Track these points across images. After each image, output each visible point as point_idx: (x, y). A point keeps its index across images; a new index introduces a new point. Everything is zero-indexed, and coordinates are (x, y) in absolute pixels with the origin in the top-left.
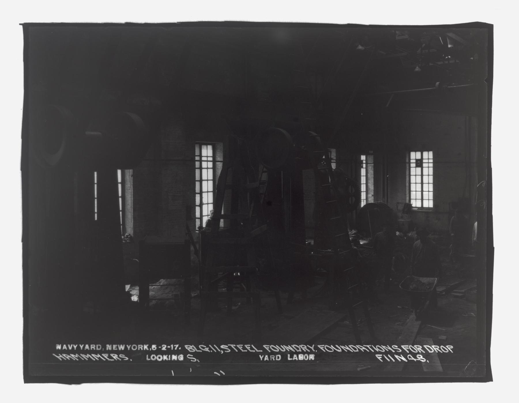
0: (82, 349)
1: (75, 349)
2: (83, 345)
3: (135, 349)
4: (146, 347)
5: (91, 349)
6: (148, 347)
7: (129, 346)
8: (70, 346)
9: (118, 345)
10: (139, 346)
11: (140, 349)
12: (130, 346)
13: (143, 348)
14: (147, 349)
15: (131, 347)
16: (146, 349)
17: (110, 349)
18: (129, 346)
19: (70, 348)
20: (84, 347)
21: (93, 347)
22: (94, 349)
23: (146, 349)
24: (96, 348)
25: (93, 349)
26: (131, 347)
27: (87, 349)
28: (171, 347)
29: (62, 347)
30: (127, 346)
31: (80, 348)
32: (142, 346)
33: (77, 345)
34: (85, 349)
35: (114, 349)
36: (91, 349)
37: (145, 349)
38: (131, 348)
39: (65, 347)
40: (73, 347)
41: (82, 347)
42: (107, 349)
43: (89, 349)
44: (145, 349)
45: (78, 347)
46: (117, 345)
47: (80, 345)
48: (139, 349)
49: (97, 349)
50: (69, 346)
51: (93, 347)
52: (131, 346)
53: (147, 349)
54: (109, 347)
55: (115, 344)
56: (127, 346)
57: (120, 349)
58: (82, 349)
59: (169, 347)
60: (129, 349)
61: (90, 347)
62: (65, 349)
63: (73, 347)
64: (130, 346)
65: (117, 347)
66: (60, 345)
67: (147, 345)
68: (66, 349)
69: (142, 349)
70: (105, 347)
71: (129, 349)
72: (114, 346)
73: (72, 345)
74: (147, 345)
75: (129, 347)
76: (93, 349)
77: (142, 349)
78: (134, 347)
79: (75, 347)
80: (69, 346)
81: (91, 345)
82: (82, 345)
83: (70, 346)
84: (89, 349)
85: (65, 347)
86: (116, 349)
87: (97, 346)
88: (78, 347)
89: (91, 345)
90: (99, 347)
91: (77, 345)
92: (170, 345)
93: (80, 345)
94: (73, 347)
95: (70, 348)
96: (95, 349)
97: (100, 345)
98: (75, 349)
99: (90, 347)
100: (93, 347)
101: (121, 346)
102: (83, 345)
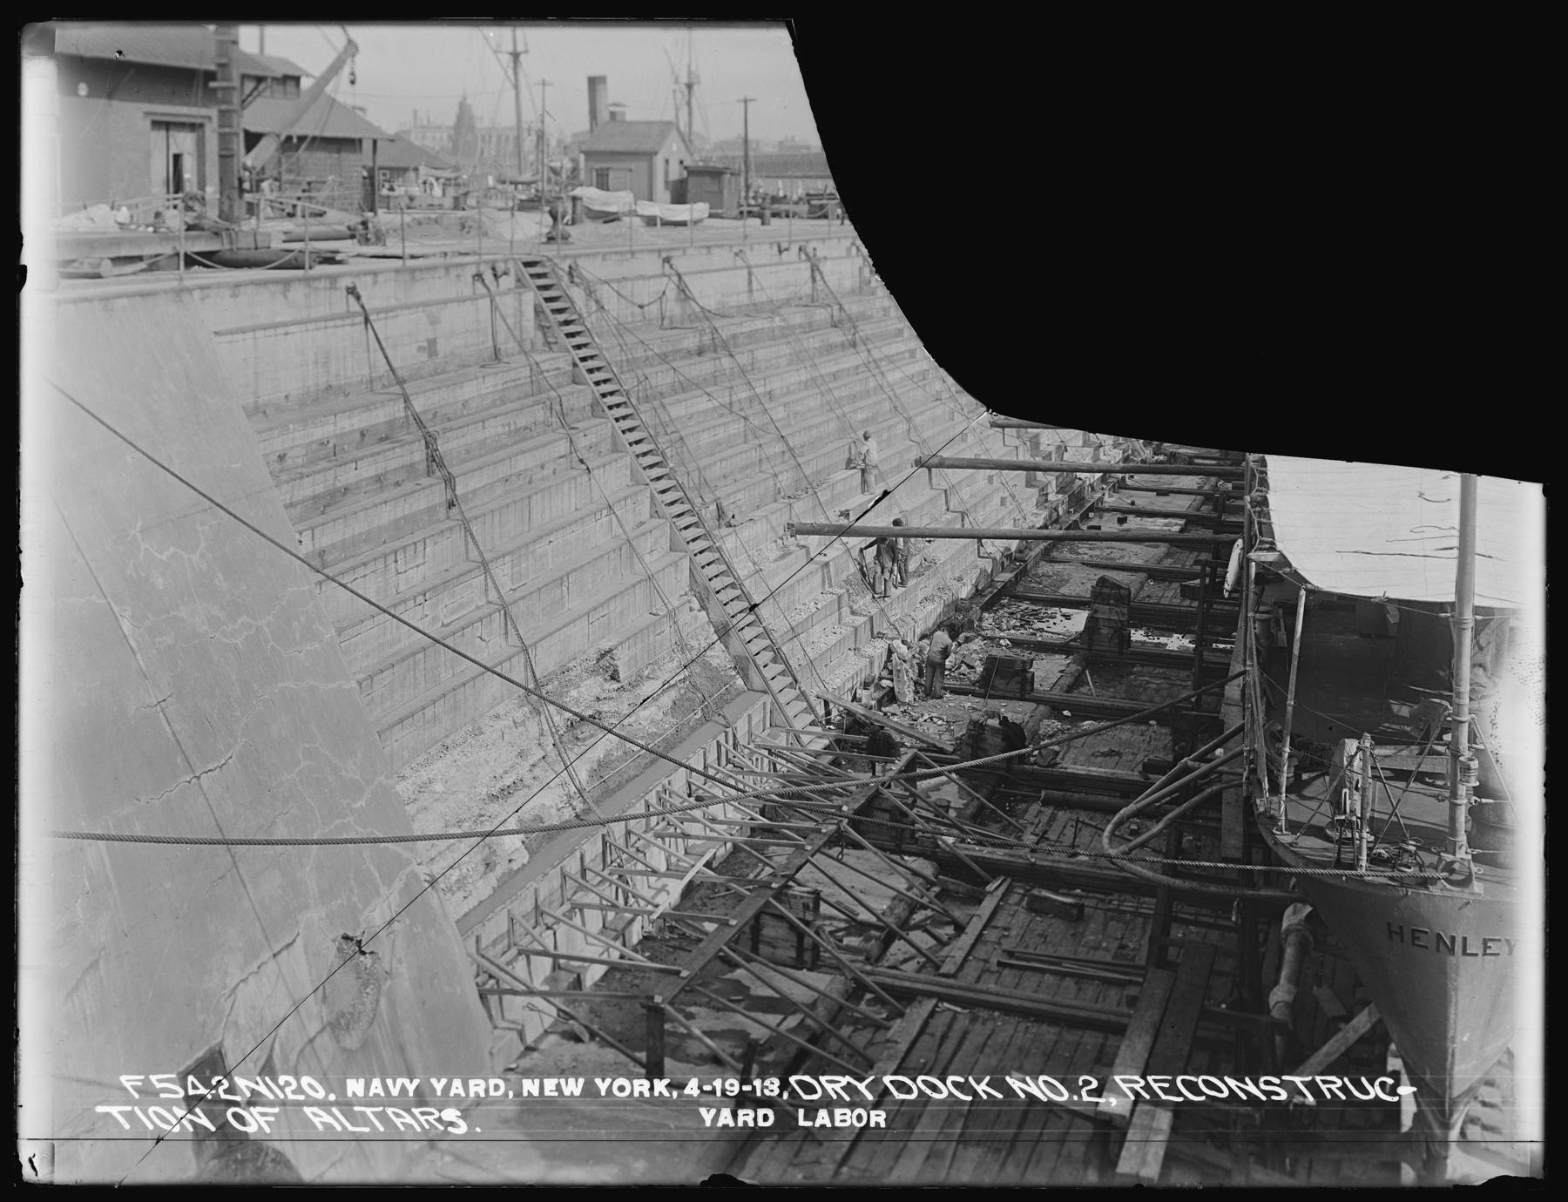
0: (439, 1093)
2: (444, 1081)
5: (472, 1095)
6: (669, 1086)
7: (603, 1080)
10: (636, 1082)
12: (608, 1081)
13: (652, 1089)
14: (666, 1094)
17: (536, 1093)
18: (603, 1080)
19: (395, 1092)
20: (447, 1088)
21: (476, 1089)
24: (487, 1091)
27: (457, 1095)
29: (367, 1087)
30: (598, 1081)
32: (647, 1084)
33: (416, 1082)
34: (452, 1094)
35: (547, 1093)
37: (656, 1094)
38: (609, 1089)
41: (439, 1086)
43: (463, 1095)
44: (656, 1094)
46: (555, 1081)
47: (434, 1081)
48: (636, 1094)
52: (614, 1080)
53: (666, 1094)
55: (550, 1076)
56: (598, 1081)
57: (567, 1092)
58: (439, 1093)
59: (747, 1088)
60: (603, 1093)
62: (376, 1095)
63: (404, 1089)
65: (558, 1088)
66: (362, 1081)
67: (666, 1081)
68: (382, 1094)
69: (647, 1094)
70: (518, 1094)
71: (603, 1093)
72: (550, 1084)
73: (400, 1081)
75: (602, 1086)
77: (647, 1094)
78: (622, 1089)
79: (411, 1088)
80: (389, 1082)
81: (472, 1082)
84: (463, 1095)
86: (556, 1094)
87: (492, 1082)
89: (472, 1082)
90: (497, 1087)
91: (416, 1082)
92: (751, 1083)
94: (404, 1089)
95: (395, 1092)
97: (501, 1083)
101: (572, 1081)
102: (444, 1081)
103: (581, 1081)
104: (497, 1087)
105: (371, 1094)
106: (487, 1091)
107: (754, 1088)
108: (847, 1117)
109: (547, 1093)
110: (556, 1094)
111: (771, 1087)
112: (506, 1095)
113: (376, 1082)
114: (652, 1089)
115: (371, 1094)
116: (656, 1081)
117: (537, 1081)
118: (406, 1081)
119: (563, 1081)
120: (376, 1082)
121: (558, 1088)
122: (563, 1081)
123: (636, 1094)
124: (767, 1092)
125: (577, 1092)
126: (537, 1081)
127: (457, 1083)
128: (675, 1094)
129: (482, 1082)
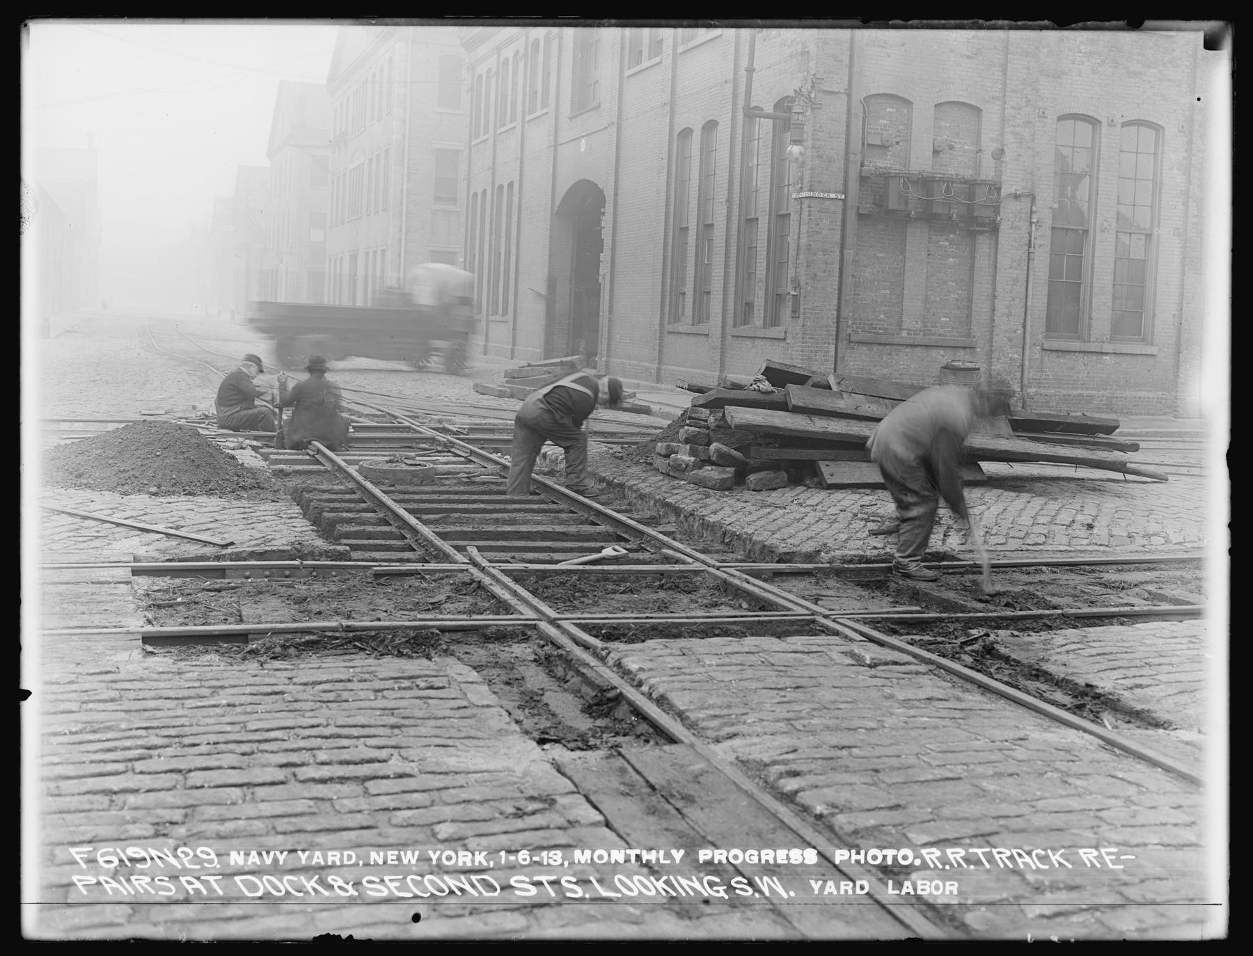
11: (464, 863)
12: (438, 853)
13: (473, 861)
14: (485, 864)
15: (441, 854)
16: (480, 862)
21: (334, 858)
23: (480, 862)
24: (341, 860)
26: (441, 854)
28: (542, 858)
30: (431, 853)
35: (389, 862)
38: (439, 859)
43: (323, 863)
46: (396, 852)
49: (346, 862)
51: (334, 858)
57: (405, 862)
60: (434, 862)
61: (325, 858)
63: (276, 860)
64: (438, 853)
67: (484, 853)
71: (434, 862)
73: (272, 853)
74: (484, 853)
78: (449, 858)
86: (396, 863)
87: (346, 853)
89: (330, 853)
90: (350, 857)
94: (276, 860)
95: (268, 861)
98: (281, 863)
99: (325, 858)
101: (409, 853)
103: (417, 853)
104: (350, 857)
108: (927, 887)
110: (396, 863)
114: (473, 861)
118: (278, 853)
120: (254, 853)
121: (399, 858)
122: (402, 853)
124: (551, 862)
125: (413, 862)
128: (492, 864)
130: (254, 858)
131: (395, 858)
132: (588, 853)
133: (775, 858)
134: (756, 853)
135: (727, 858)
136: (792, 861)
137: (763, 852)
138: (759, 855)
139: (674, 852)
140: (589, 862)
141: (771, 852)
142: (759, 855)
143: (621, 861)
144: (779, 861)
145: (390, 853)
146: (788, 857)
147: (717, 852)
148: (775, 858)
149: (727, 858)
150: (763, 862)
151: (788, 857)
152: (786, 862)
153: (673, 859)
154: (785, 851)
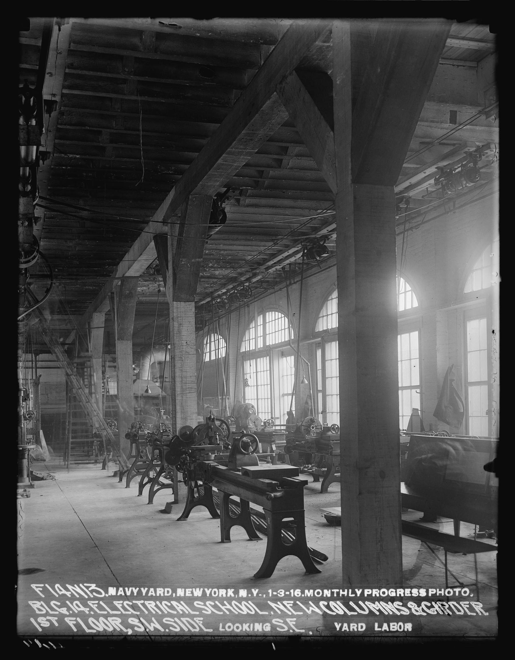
0: (144, 594)
1: (135, 594)
2: (146, 589)
3: (217, 595)
4: (230, 592)
5: (158, 595)
7: (208, 590)
8: (128, 590)
9: (192, 588)
12: (210, 590)
13: (227, 593)
16: (230, 596)
17: (182, 595)
18: (208, 590)
19: (128, 593)
22: (162, 595)
23: (230, 596)
24: (164, 593)
25: (160, 594)
31: (142, 593)
33: (138, 589)
35: (187, 595)
36: (158, 595)
37: (228, 596)
38: (211, 594)
39: (121, 592)
40: (132, 591)
41: (144, 591)
42: (178, 595)
43: (154, 595)
44: (228, 596)
45: (140, 592)
46: (191, 590)
47: (142, 589)
48: (220, 596)
49: (166, 594)
50: (126, 589)
53: (233, 595)
54: (180, 592)
58: (144, 594)
60: (208, 595)
61: (156, 592)
62: (121, 595)
63: (132, 592)
66: (115, 588)
68: (123, 594)
71: (208, 595)
72: (188, 591)
73: (130, 589)
74: (233, 590)
75: (208, 592)
76: (160, 594)
78: (215, 593)
79: (135, 591)
80: (126, 589)
82: (144, 589)
83: (128, 590)
84: (154, 595)
85: (121, 591)
86: (191, 595)
87: (166, 590)
88: (140, 592)
89: (158, 589)
90: (168, 592)
91: (138, 589)
93: (142, 589)
94: (132, 592)
95: (128, 593)
96: (162, 595)
98: (135, 594)
100: (160, 591)
101: (198, 589)
102: (146, 589)
103: (202, 589)
104: (168, 592)
105: (119, 594)
106: (164, 593)
107: (290, 593)
109: (187, 595)
110: (191, 595)
111: (281, 593)
112: (172, 594)
113: (121, 589)
114: (227, 593)
115: (119, 594)
116: (229, 590)
117: (183, 590)
118: (134, 589)
119: (194, 589)
120: (121, 589)
123: (220, 596)
125: (200, 595)
126: (183, 590)
127: (152, 590)
129: (162, 589)
130: (121, 592)
131: (190, 592)
132: (311, 591)
133: (404, 593)
134: (394, 590)
135: (379, 593)
136: (413, 595)
137: (398, 590)
138: (396, 592)
139: (356, 590)
140: (312, 595)
141: (402, 590)
142: (396, 592)
143: (329, 595)
144: (406, 595)
145: (187, 590)
146: (411, 593)
147: (374, 590)
148: (404, 593)
149: (379, 593)
150: (398, 595)
151: (411, 593)
152: (410, 595)
153: (356, 594)
154: (410, 590)
